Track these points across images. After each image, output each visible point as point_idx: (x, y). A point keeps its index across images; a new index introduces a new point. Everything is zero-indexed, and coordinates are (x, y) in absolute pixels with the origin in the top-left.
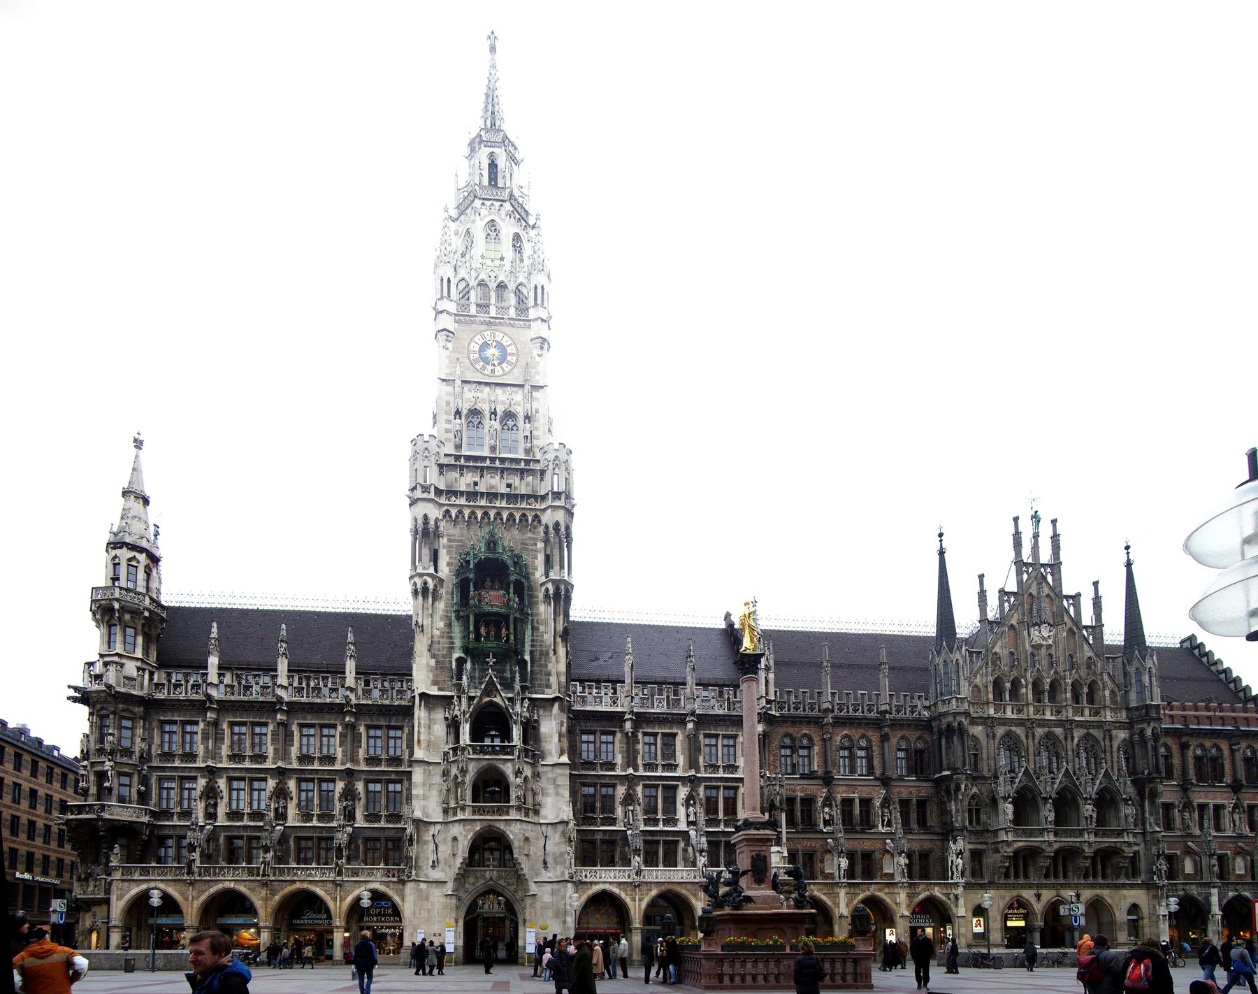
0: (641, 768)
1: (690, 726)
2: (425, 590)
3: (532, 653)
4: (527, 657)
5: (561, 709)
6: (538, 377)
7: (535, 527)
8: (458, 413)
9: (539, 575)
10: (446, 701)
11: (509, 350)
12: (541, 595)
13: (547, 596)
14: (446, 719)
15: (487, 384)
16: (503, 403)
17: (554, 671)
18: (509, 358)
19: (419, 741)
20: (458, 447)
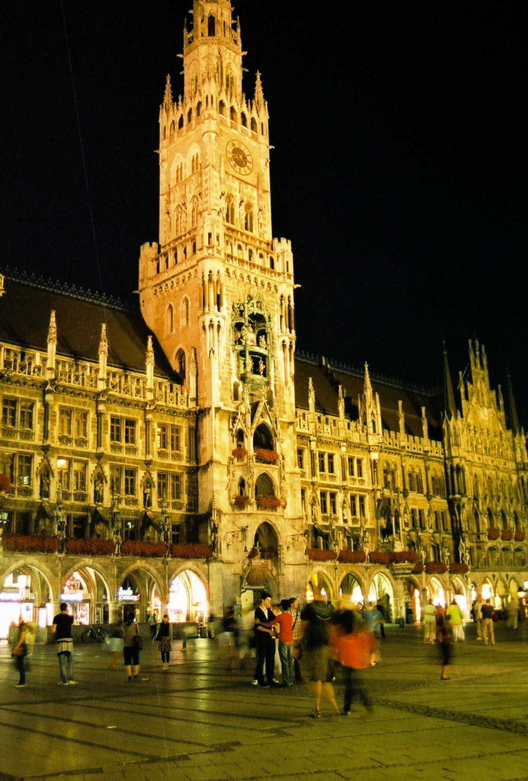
1: (344, 449)
2: (219, 326)
3: (275, 385)
4: (273, 389)
8: (223, 194)
10: (233, 417)
13: (284, 346)
14: (230, 430)
15: (238, 179)
18: (248, 164)
19: (215, 446)
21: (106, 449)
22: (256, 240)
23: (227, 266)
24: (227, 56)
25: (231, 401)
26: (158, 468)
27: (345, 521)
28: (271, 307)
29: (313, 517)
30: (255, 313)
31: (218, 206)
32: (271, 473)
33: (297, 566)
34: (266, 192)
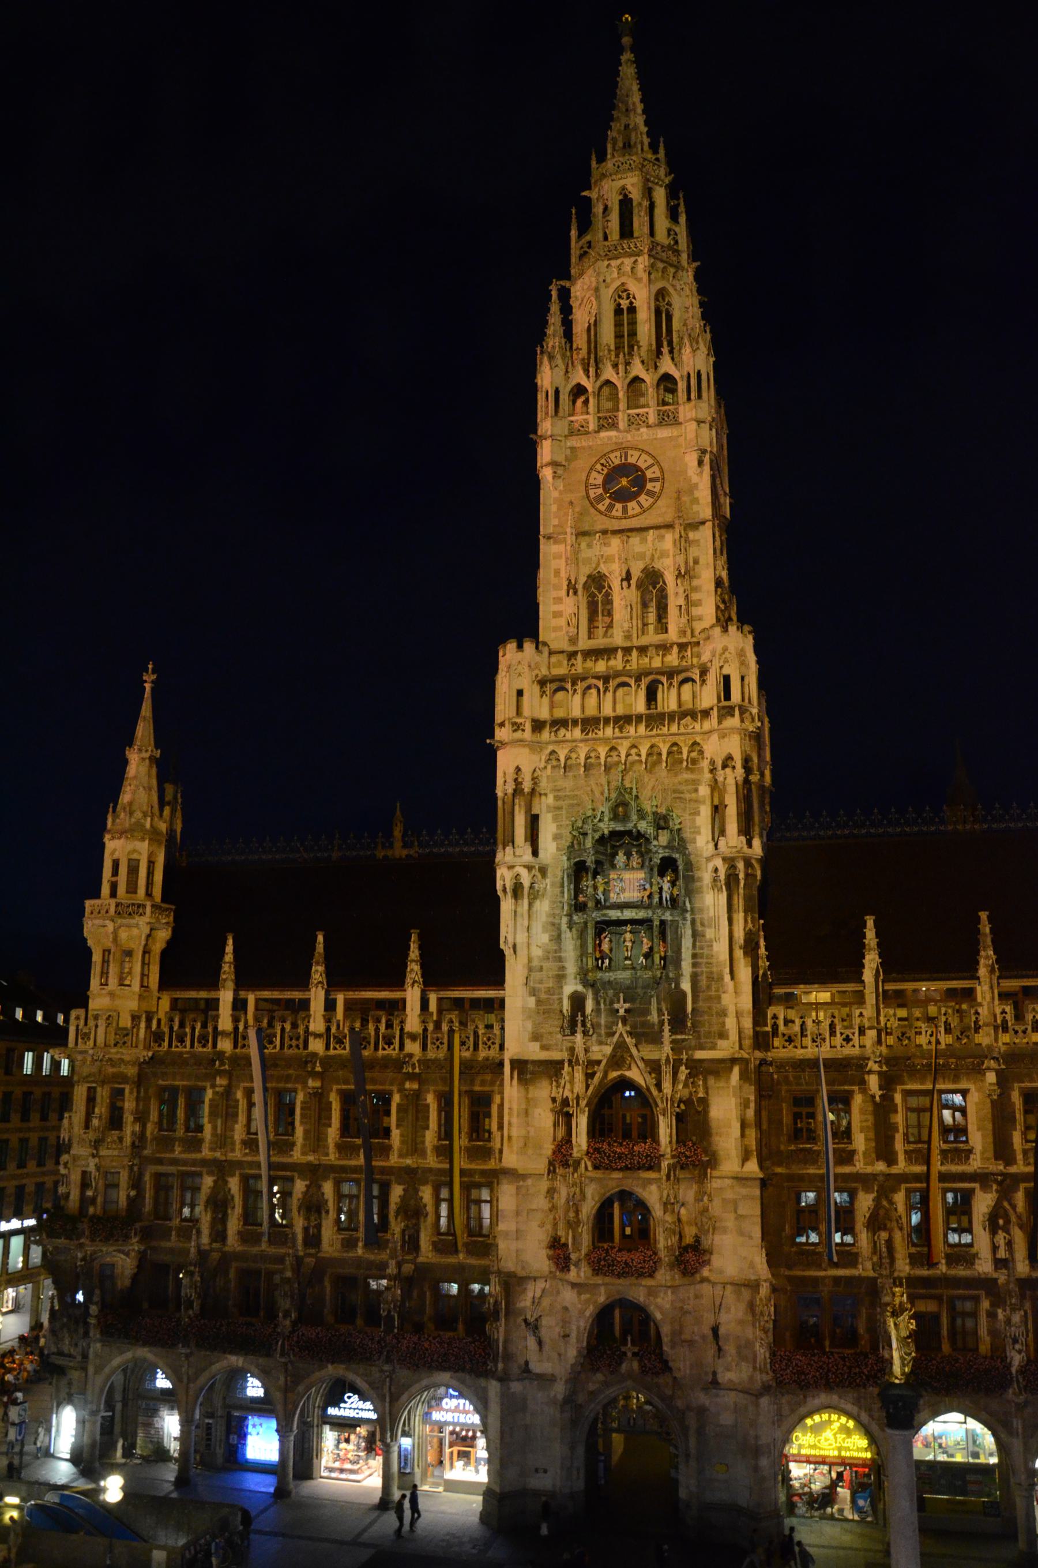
0: (901, 1157)
3: (695, 979)
4: (686, 986)
5: (744, 1076)
6: (695, 508)
7: (694, 761)
9: (702, 842)
10: (552, 1069)
11: (649, 474)
12: (707, 877)
14: (554, 1100)
15: (615, 532)
16: (642, 556)
17: (731, 1010)
18: (649, 486)
20: (573, 640)
21: (327, 1155)
22: (671, 647)
23: (550, 748)
24: (615, 275)
25: (559, 1036)
26: (432, 1178)
27: (1000, 1264)
28: (688, 796)
29: (875, 1259)
30: (606, 832)
31: (561, 616)
32: (640, 1190)
33: (741, 1395)
34: (703, 523)
